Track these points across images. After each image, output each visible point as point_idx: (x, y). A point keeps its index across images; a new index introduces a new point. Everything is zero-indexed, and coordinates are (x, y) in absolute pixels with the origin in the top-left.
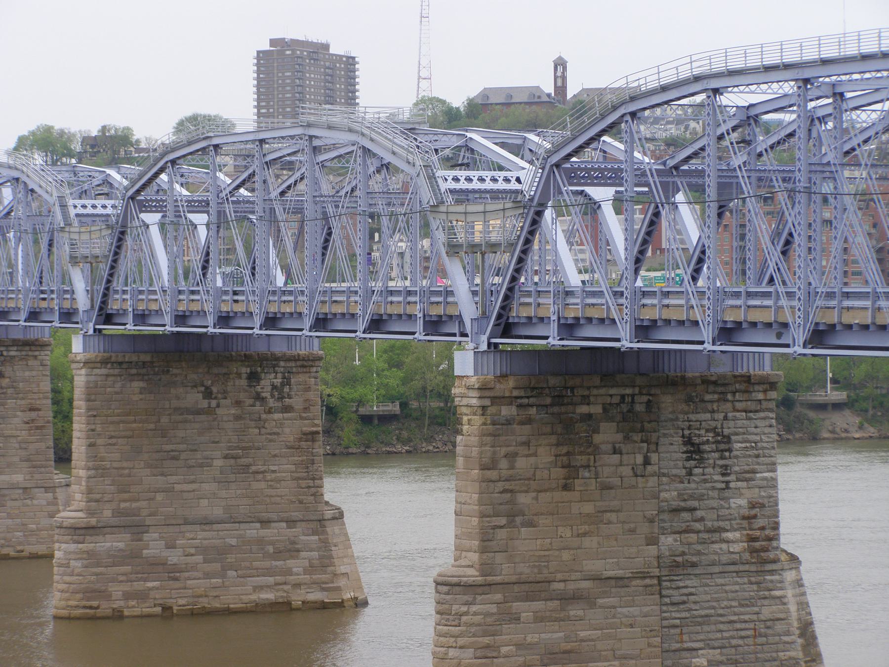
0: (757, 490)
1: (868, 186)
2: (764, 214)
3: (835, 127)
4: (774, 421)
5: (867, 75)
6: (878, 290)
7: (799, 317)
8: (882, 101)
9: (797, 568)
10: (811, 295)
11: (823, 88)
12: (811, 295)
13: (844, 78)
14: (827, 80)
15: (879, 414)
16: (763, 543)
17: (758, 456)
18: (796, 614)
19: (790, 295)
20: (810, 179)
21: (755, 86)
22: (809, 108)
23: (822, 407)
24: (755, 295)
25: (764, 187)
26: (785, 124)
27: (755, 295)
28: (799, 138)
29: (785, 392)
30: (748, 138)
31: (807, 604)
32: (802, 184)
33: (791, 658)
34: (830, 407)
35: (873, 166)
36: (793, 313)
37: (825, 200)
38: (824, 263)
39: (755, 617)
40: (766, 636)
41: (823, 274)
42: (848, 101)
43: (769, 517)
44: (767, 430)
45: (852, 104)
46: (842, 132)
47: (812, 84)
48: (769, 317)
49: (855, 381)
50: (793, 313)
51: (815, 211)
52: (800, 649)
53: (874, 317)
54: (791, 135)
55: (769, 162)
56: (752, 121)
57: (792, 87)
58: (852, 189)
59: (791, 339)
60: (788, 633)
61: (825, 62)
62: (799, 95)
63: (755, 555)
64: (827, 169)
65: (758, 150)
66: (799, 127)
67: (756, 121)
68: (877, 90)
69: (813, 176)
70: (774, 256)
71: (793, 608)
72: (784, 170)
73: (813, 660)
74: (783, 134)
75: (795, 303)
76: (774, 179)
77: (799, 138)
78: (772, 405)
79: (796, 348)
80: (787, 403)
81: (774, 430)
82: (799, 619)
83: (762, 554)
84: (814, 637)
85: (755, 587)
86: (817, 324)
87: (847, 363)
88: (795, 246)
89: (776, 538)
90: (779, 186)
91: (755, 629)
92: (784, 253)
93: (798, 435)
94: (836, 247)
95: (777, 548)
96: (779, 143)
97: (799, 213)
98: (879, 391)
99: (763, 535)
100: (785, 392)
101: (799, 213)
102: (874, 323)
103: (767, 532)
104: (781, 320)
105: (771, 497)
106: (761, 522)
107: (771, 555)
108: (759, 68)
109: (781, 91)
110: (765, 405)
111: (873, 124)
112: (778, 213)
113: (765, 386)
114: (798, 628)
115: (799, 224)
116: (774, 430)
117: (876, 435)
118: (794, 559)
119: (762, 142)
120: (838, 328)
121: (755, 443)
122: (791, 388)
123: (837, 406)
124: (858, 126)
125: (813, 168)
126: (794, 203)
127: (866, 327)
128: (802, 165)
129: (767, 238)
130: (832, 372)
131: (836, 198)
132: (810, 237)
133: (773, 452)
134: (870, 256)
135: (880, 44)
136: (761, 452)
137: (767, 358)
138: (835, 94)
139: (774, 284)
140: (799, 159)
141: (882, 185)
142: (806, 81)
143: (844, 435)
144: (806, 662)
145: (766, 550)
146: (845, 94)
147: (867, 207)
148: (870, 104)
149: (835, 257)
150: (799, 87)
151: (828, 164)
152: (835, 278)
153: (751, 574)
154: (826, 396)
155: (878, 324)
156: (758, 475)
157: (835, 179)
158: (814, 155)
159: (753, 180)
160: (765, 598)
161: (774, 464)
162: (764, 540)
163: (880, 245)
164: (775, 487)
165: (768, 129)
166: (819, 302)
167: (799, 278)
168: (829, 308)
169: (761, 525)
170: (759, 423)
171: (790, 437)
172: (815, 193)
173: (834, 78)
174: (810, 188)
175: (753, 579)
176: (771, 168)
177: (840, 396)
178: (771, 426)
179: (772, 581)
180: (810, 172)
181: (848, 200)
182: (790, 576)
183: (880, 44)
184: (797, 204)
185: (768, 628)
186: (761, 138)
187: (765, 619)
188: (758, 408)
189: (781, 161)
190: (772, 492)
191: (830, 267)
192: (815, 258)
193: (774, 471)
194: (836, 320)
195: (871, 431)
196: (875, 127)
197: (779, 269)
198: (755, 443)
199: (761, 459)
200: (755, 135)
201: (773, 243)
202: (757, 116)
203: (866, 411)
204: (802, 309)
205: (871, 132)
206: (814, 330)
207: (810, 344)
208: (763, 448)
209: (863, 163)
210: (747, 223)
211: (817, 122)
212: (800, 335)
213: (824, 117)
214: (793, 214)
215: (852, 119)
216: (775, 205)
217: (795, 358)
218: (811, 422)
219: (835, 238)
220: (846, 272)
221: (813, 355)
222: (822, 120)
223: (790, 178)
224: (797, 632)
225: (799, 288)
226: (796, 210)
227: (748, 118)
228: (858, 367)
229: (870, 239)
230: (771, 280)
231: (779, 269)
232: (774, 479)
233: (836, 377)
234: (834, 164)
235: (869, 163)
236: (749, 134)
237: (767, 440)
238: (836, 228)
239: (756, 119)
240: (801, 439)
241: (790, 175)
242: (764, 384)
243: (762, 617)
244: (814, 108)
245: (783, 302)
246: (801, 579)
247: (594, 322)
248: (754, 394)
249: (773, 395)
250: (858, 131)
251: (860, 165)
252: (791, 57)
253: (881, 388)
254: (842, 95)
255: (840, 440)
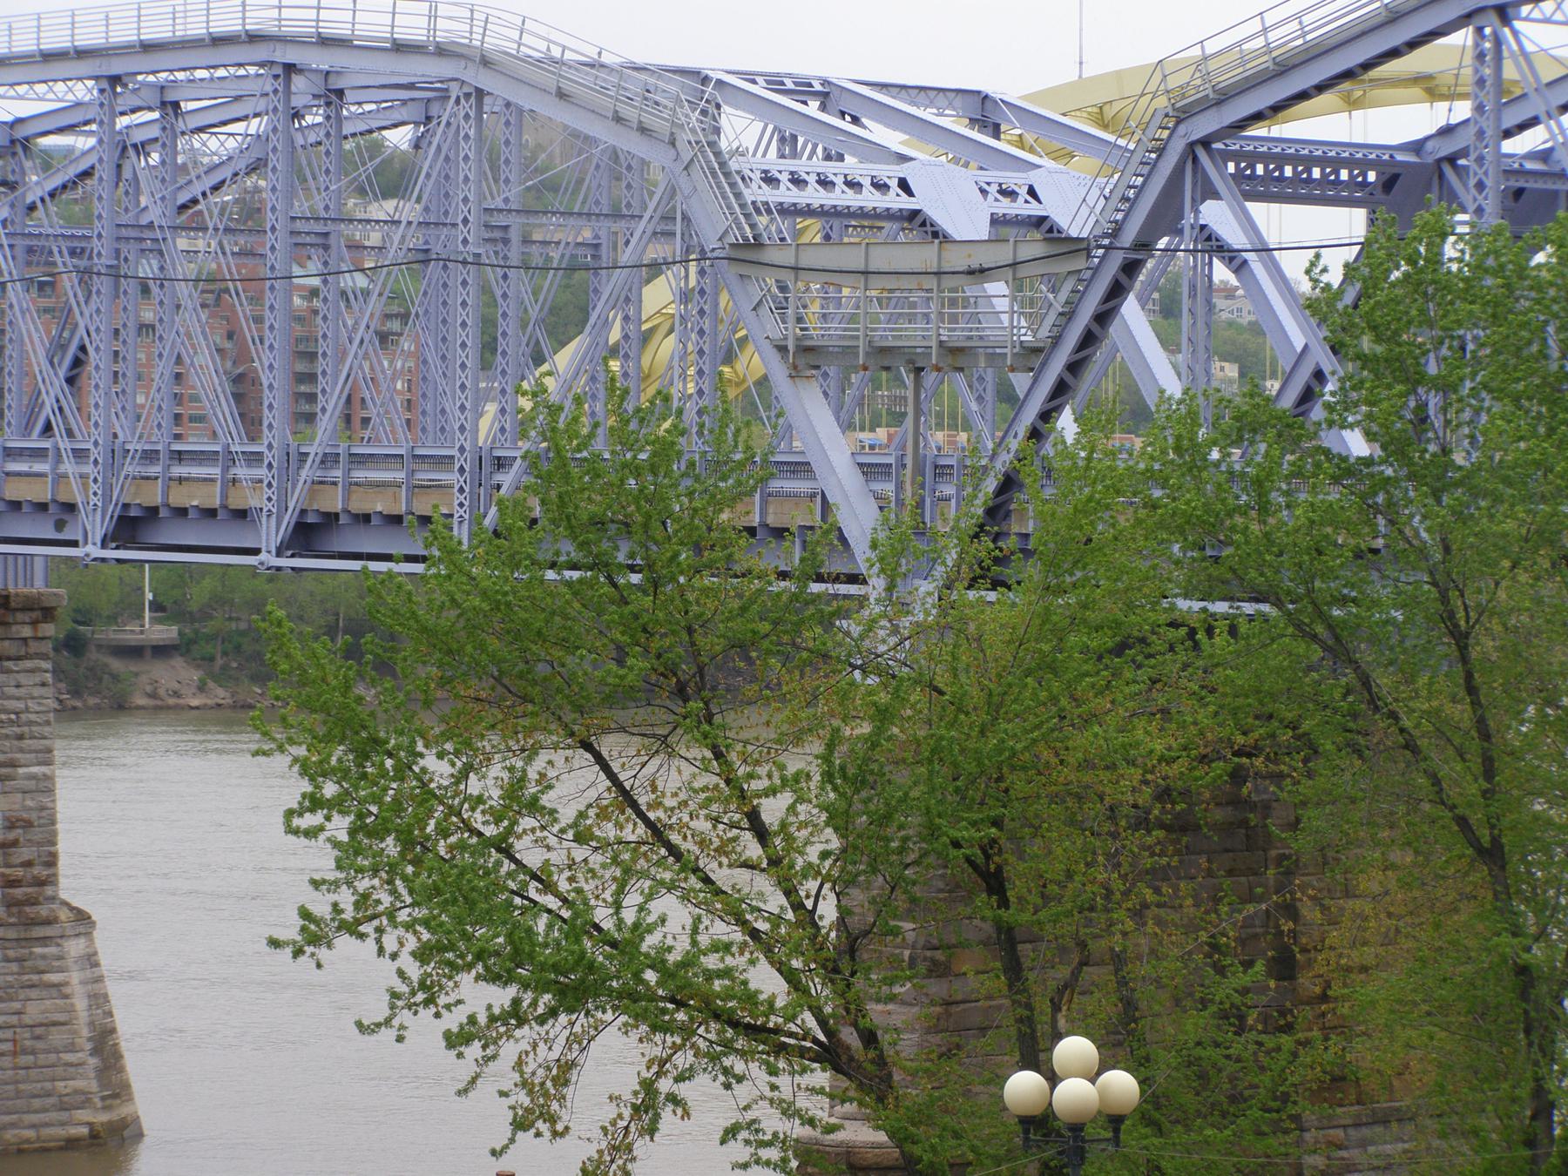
0: (20, 796)
1: (219, 266)
2: (38, 311)
3: (163, 162)
4: (48, 675)
5: (221, 72)
6: (233, 449)
7: (95, 494)
8: (245, 118)
9: (88, 935)
10: (116, 454)
11: (144, 93)
12: (116, 454)
13: (180, 76)
14: (151, 78)
15: (235, 665)
16: (30, 890)
17: (20, 737)
18: (85, 1014)
19: (80, 455)
20: (118, 251)
21: (26, 87)
22: (118, 127)
23: (134, 652)
24: (18, 454)
25: (38, 264)
26: (77, 153)
27: (18, 454)
28: (101, 179)
29: (71, 625)
30: (11, 178)
31: (106, 996)
32: (103, 261)
33: (77, 1092)
34: (148, 652)
35: (227, 230)
36: (85, 486)
37: (145, 290)
38: (140, 399)
39: (14, 1019)
40: (33, 1052)
41: (138, 418)
42: (187, 118)
43: (40, 844)
44: (37, 692)
45: (194, 122)
46: (174, 171)
47: (125, 86)
48: (41, 492)
49: (194, 607)
50: (85, 486)
51: (125, 309)
52: (92, 1075)
53: (224, 496)
54: (87, 174)
55: (48, 222)
56: (19, 150)
57: (90, 91)
58: (191, 270)
59: (80, 532)
60: (72, 1048)
61: (147, 47)
62: (102, 105)
63: (15, 910)
64: (147, 234)
65: (29, 200)
66: (101, 160)
67: (25, 149)
68: (237, 98)
69: (124, 247)
70: (53, 387)
71: (80, 1004)
72: (73, 236)
73: (115, 1096)
74: (72, 171)
75: (88, 469)
76: (55, 250)
77: (101, 179)
78: (47, 647)
79: (89, 548)
80: (73, 645)
81: (49, 691)
82: (91, 1024)
83: (27, 909)
84: (117, 1056)
85: (14, 967)
86: (126, 506)
87: (180, 576)
88: (90, 368)
89: (51, 880)
90: (64, 264)
91: (14, 1041)
92: (70, 381)
93: (92, 701)
94: (162, 371)
95: (53, 899)
96: (64, 187)
97: (98, 311)
98: (233, 626)
99: (29, 876)
100: (71, 625)
101: (98, 311)
102: (224, 507)
103: (36, 870)
104: (62, 498)
105: (43, 809)
106: (25, 853)
107: (43, 910)
108: (33, 56)
109: (70, 97)
110: (34, 647)
111: (230, 158)
112: (62, 311)
113: (36, 615)
114: (90, 1039)
115: (98, 330)
116: (49, 691)
117: (230, 701)
118: (82, 917)
119: (36, 184)
120: (163, 513)
121: (17, 713)
122: (80, 618)
123: (161, 651)
124: (206, 160)
125: (124, 232)
126: (90, 292)
127: (211, 513)
128: (104, 227)
129: (42, 354)
130: (154, 590)
131: (162, 286)
132: (116, 353)
133: (46, 730)
134: (219, 389)
135: (244, 19)
136: (26, 729)
137: (39, 565)
138: (164, 104)
139: (53, 436)
140: (100, 217)
141: (245, 265)
142: (115, 80)
143: (172, 701)
144: (103, 1098)
145: (33, 901)
146: (182, 104)
147: (218, 299)
148: (225, 123)
149: (159, 390)
150: (102, 91)
151: (150, 226)
152: (159, 426)
153: (7, 944)
154: (142, 632)
155: (232, 507)
156: (21, 771)
157: (161, 253)
158: (126, 210)
159: (19, 251)
160: (32, 986)
161: (49, 751)
162: (30, 885)
163: (240, 371)
164: (50, 791)
165: (47, 162)
166: (130, 468)
167: (96, 424)
168: (148, 478)
169: (26, 857)
170: (23, 679)
171: (78, 704)
172: (126, 277)
173: (163, 75)
174: (117, 267)
175: (11, 953)
176: (50, 231)
177: (165, 633)
178: (44, 685)
179: (44, 957)
180: (118, 239)
181: (183, 290)
182: (75, 947)
183: (244, 19)
184: (94, 296)
185: (38, 1038)
186: (34, 178)
187: (30, 1022)
188: (23, 653)
189: (69, 220)
190: (45, 800)
191: (152, 407)
192: (124, 391)
193: (49, 763)
194: (159, 500)
195: (221, 694)
196: (233, 163)
197: (60, 409)
198: (17, 713)
199: (27, 743)
200: (24, 173)
201: (52, 363)
202: (27, 139)
203: (212, 659)
204: (275, 484)
205: (226, 173)
206: (120, 517)
207: (113, 540)
208: (30, 723)
209: (211, 226)
210: (8, 328)
211: (131, 152)
212: (97, 526)
213: (143, 144)
214: (87, 314)
215: (192, 149)
216: (58, 297)
217: (86, 566)
218: (115, 677)
219: (160, 355)
220: (177, 417)
221: (118, 561)
222: (142, 148)
223: (83, 250)
224: (89, 1046)
225: (96, 443)
226: (93, 307)
227: (13, 142)
228: (198, 583)
229: (223, 359)
230: (48, 429)
231: (60, 409)
232: (49, 778)
233: (161, 599)
234: (161, 227)
235: (221, 227)
236: (13, 171)
237: (38, 708)
238: (161, 338)
239: (26, 144)
240: (98, 708)
241: (83, 244)
242: (32, 609)
243: (27, 1020)
244: (127, 127)
245: (68, 467)
246: (95, 954)
247: (25, 509)
248: (14, 628)
249: (48, 629)
250: (202, 170)
251: (205, 229)
252: (89, 37)
253: (238, 619)
254: (176, 105)
255: (164, 709)
